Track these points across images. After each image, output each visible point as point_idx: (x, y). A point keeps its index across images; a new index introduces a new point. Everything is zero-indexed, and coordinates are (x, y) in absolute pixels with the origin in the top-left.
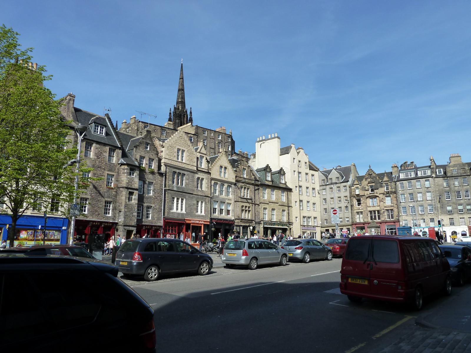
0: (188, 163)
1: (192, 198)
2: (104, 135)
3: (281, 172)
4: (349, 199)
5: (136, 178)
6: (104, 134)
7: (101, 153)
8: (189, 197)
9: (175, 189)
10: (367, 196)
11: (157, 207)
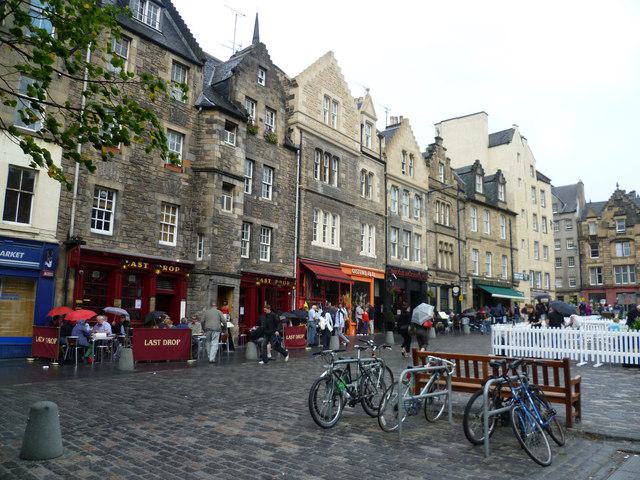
0: (344, 131)
2: (157, 28)
3: (498, 178)
4: (576, 244)
5: (240, 149)
6: (157, 24)
7: (152, 69)
9: (320, 191)
10: (611, 239)
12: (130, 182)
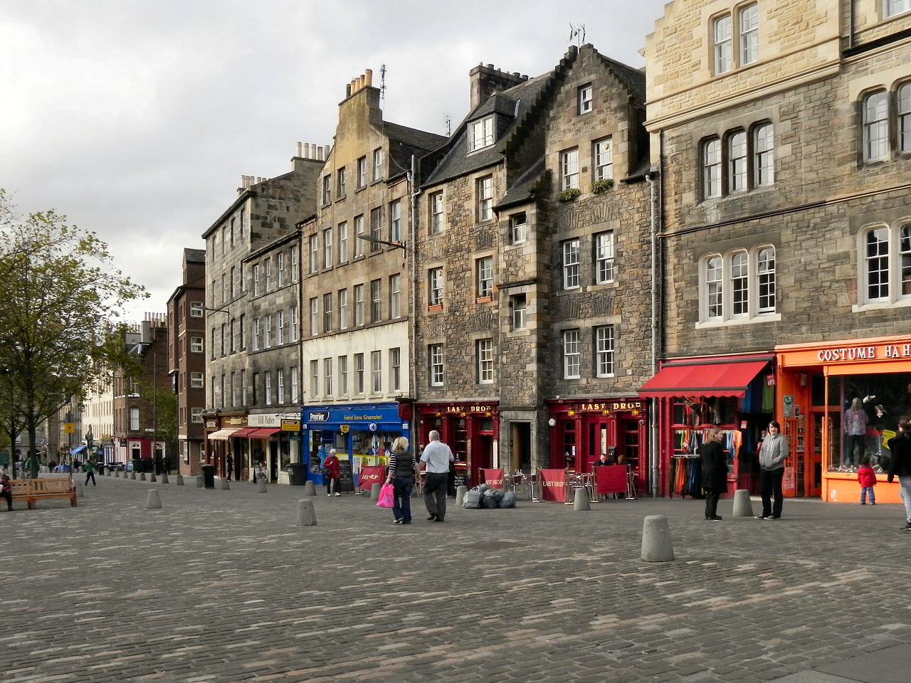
1: (827, 221)
5: (529, 243)
8: (801, 228)
11: (634, 321)
12: (450, 332)
